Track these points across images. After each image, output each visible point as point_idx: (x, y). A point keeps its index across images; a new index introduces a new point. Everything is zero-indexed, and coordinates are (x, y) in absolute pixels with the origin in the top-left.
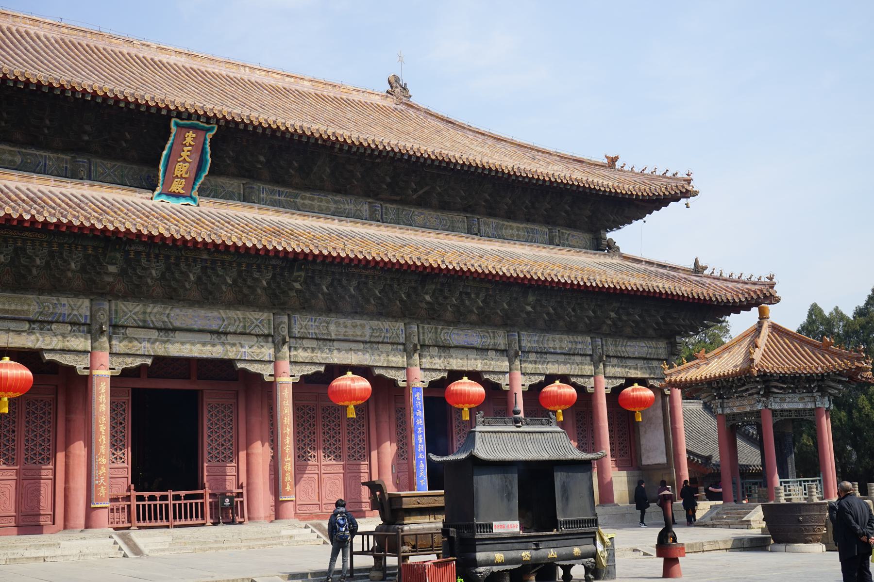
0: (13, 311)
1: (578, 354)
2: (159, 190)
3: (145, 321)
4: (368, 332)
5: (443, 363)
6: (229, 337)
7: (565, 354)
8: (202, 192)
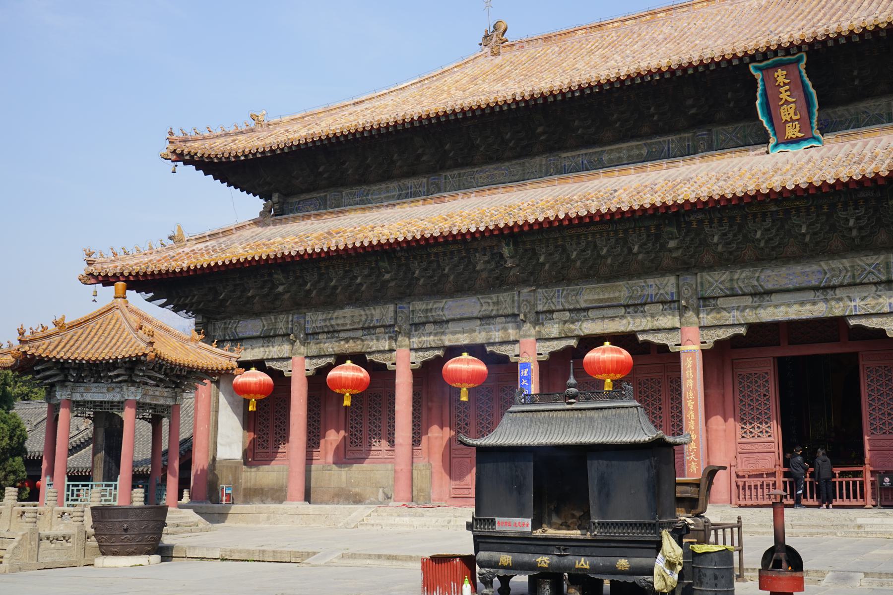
0: (607, 300)
2: (773, 141)
3: (732, 289)
5: (432, 341)
6: (838, 291)
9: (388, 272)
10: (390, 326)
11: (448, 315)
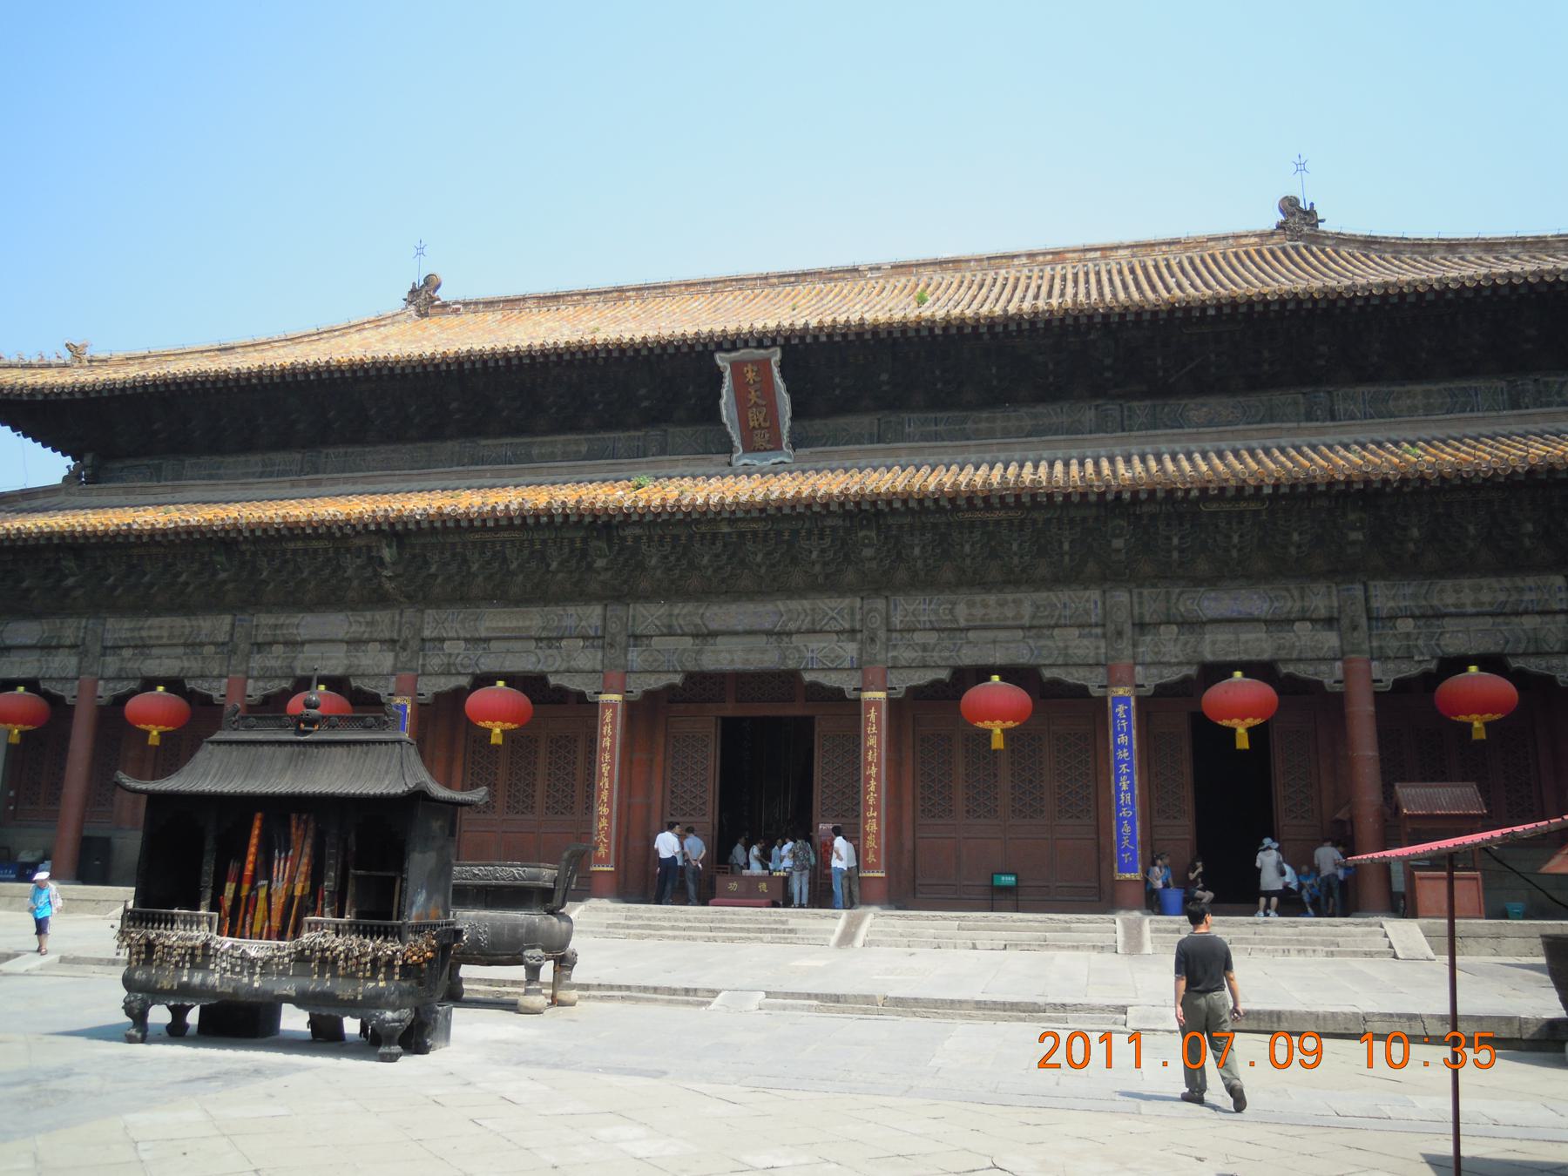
0: (514, 629)
1: (1526, 612)
3: (670, 627)
4: (1027, 610)
6: (794, 638)
7: (1492, 614)
8: (795, 445)
9: (225, 570)
10: (223, 644)
11: (303, 634)
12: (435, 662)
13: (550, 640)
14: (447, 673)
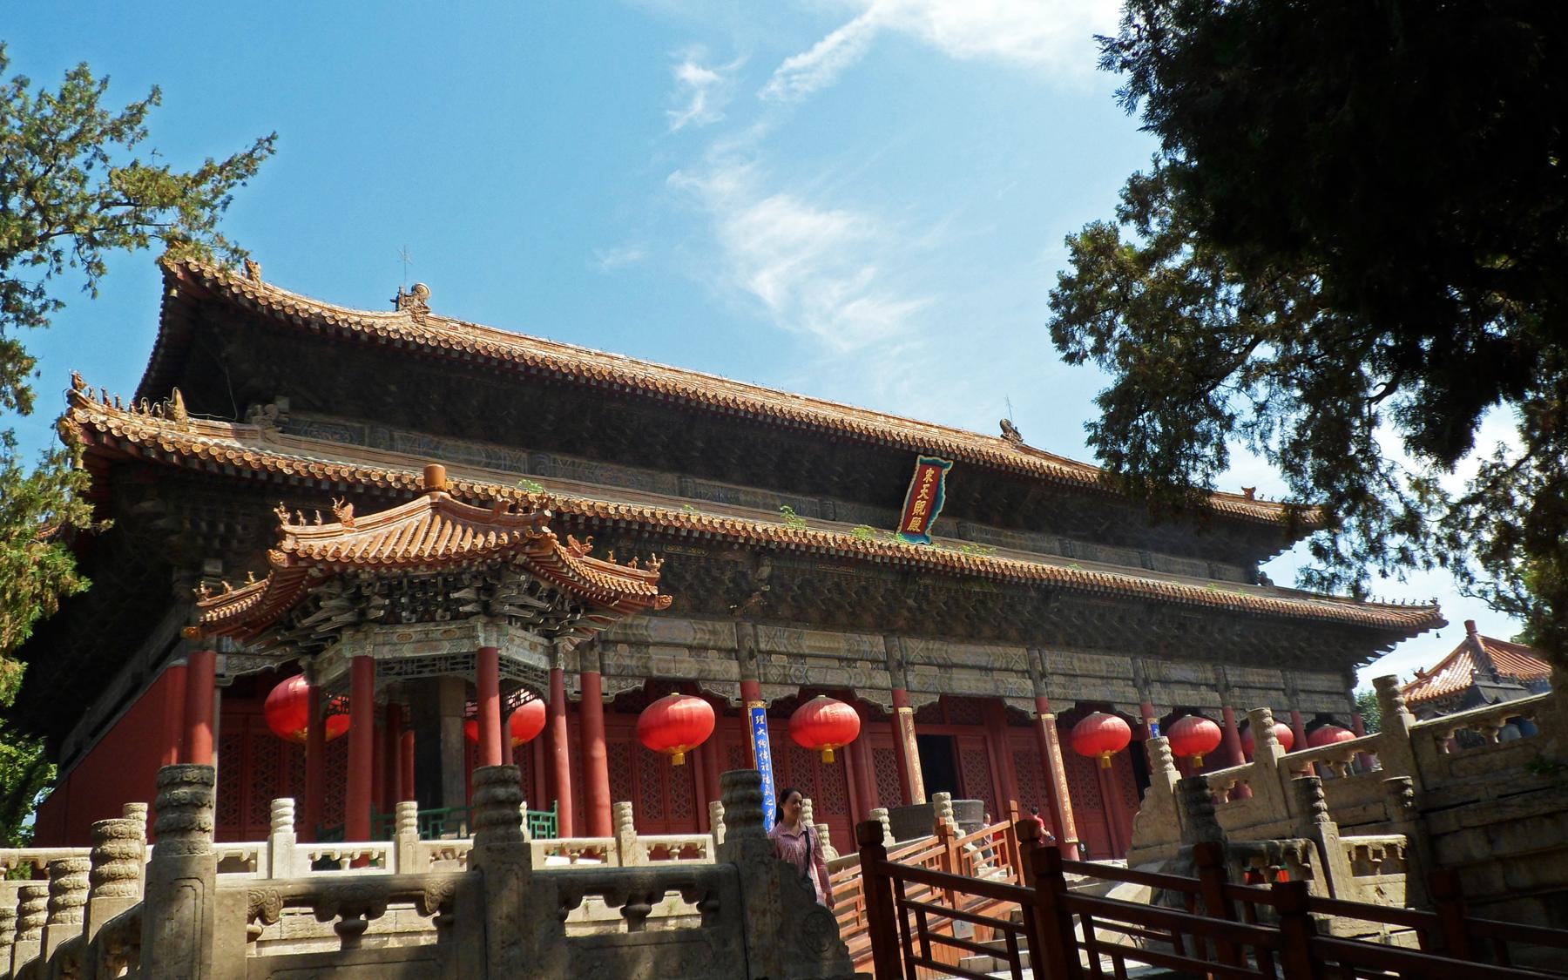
8: (935, 532)
11: (654, 636)
12: (774, 673)
13: (848, 661)
14: (783, 683)
